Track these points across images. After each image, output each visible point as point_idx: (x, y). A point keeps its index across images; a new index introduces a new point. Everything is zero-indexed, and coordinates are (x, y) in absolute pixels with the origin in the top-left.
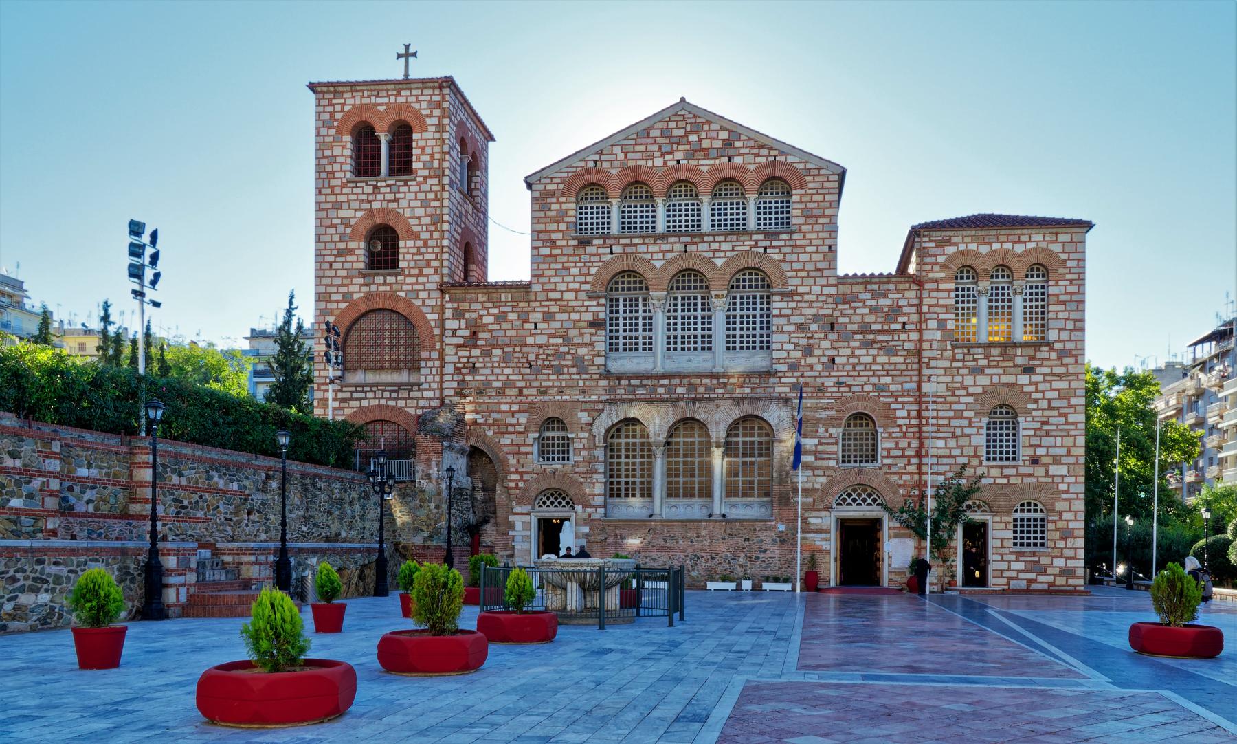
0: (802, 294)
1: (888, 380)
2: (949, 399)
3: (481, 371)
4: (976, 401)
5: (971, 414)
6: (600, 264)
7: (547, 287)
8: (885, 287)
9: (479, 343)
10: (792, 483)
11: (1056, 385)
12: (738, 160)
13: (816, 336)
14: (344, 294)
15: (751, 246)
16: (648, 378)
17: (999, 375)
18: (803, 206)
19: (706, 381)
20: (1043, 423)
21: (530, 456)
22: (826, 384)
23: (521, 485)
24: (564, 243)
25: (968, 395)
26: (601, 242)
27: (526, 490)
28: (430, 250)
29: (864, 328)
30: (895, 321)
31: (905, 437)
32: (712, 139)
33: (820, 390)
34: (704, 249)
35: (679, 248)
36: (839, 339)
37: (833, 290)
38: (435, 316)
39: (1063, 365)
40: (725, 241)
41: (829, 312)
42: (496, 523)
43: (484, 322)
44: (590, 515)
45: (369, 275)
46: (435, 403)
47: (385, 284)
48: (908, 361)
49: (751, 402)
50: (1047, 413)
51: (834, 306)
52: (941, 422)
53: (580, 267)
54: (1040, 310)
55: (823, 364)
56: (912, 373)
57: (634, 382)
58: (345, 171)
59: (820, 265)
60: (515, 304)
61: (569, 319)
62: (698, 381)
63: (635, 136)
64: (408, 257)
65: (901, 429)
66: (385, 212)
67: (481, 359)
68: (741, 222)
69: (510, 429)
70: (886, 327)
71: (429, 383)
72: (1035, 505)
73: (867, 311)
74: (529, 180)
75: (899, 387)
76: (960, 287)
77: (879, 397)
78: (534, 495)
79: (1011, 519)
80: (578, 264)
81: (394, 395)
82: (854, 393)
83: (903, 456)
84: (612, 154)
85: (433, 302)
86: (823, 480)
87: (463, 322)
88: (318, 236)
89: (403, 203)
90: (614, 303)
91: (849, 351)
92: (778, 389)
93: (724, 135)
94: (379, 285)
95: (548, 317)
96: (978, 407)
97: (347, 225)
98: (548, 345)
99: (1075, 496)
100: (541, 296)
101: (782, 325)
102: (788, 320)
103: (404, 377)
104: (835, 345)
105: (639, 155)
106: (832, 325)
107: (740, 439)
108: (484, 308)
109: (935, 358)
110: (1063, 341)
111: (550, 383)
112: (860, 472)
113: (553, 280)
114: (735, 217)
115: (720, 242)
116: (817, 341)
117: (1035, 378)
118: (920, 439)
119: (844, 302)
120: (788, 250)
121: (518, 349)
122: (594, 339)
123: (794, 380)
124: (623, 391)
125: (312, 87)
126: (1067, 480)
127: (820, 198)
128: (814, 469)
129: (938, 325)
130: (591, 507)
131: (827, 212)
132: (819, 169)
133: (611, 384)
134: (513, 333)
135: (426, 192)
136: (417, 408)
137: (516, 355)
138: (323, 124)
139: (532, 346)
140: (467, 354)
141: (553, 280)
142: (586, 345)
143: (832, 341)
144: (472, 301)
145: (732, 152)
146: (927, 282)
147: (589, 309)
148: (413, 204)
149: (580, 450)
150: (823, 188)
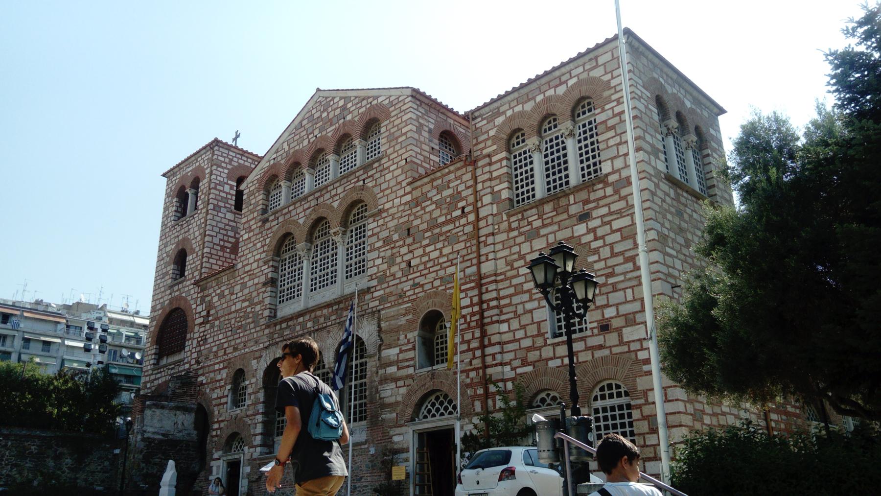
2: (509, 274)
3: (210, 340)
7: (245, 263)
8: (446, 179)
10: (380, 398)
12: (349, 117)
13: (397, 244)
15: (355, 183)
17: (554, 232)
18: (387, 133)
19: (325, 311)
20: (608, 276)
21: (225, 406)
22: (405, 290)
29: (433, 225)
30: (456, 209)
31: (469, 328)
33: (401, 296)
35: (313, 203)
36: (414, 242)
37: (408, 198)
39: (621, 199)
41: (406, 219)
44: (252, 455)
48: (468, 244)
50: (611, 262)
52: (503, 302)
55: (402, 270)
59: (399, 179)
62: (319, 313)
64: (189, 267)
65: (465, 320)
69: (218, 384)
70: (449, 217)
72: (618, 387)
73: (434, 206)
77: (445, 290)
78: (223, 441)
83: (469, 350)
86: (403, 390)
89: (191, 231)
91: (420, 252)
92: (371, 305)
93: (341, 103)
100: (241, 272)
104: (411, 248)
106: (409, 230)
109: (493, 234)
110: (619, 171)
112: (433, 375)
117: (593, 224)
118: (482, 325)
119: (417, 206)
121: (227, 318)
122: (265, 295)
123: (381, 292)
125: (164, 175)
127: (399, 121)
128: (396, 380)
129: (493, 199)
131: (404, 130)
132: (398, 98)
133: (271, 331)
138: (168, 195)
139: (234, 312)
145: (345, 113)
146: (480, 160)
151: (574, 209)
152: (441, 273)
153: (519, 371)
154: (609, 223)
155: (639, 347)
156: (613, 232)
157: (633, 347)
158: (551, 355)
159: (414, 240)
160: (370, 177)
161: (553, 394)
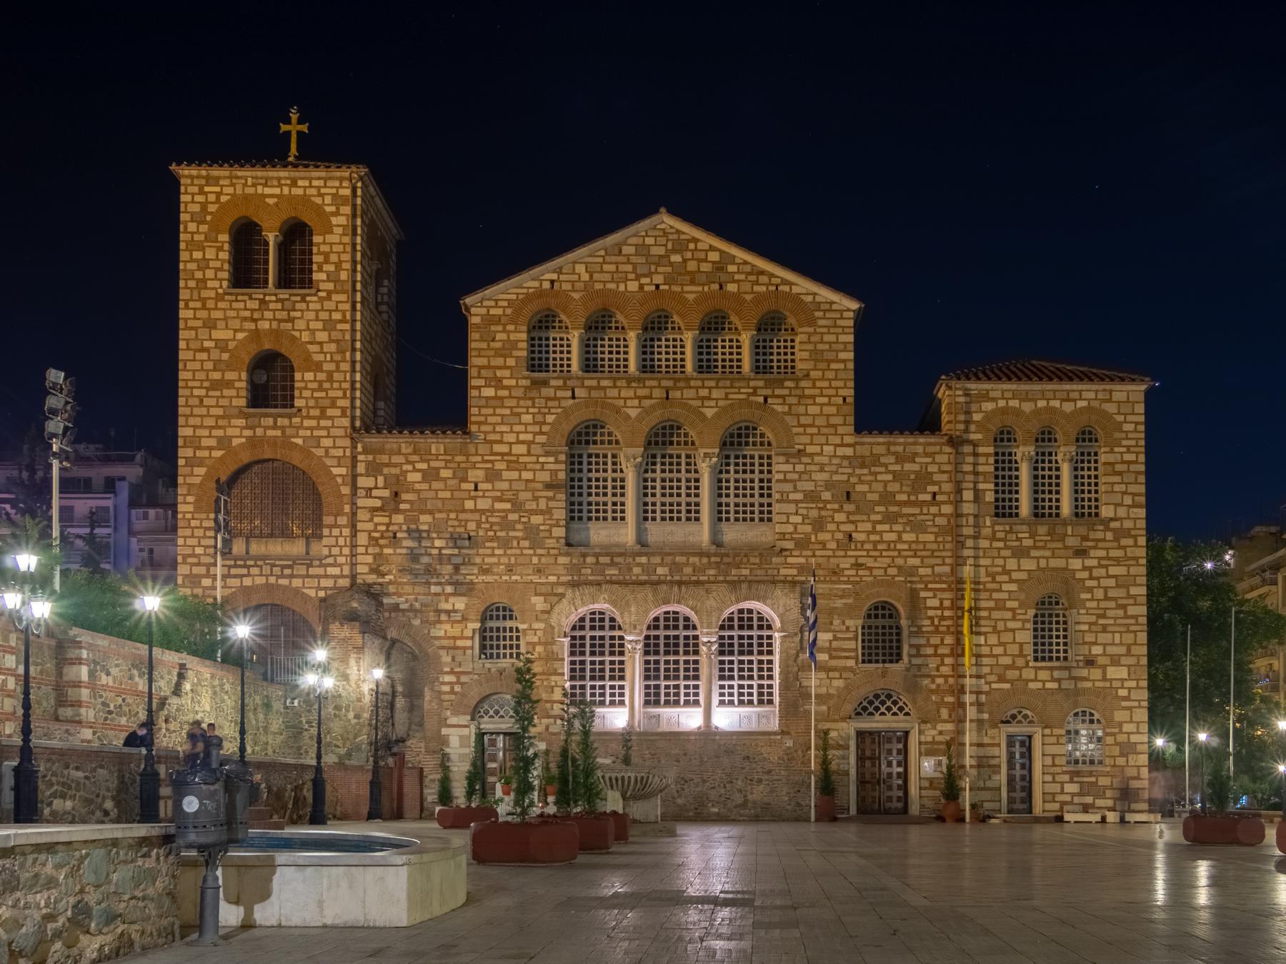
0: (812, 455)
1: (916, 561)
4: (1020, 589)
5: (1015, 604)
6: (559, 410)
7: (492, 437)
9: (402, 506)
11: (1113, 571)
12: (731, 288)
13: (829, 506)
14: (220, 439)
15: (749, 394)
16: (621, 555)
17: (1047, 558)
18: (811, 347)
20: (1099, 616)
22: (842, 566)
23: (457, 688)
24: (513, 382)
25: (1011, 581)
26: (560, 383)
27: (463, 695)
28: (336, 385)
29: (888, 498)
31: (937, 631)
32: (700, 261)
33: (835, 573)
34: (691, 396)
35: (658, 393)
36: (858, 511)
37: (849, 451)
39: (1120, 547)
40: (717, 387)
41: (845, 478)
42: (424, 737)
43: (409, 479)
45: (254, 415)
46: (344, 583)
47: (275, 427)
48: (940, 539)
49: (750, 588)
51: (850, 471)
53: (534, 414)
54: (1093, 481)
55: (838, 541)
56: (944, 554)
57: (603, 560)
58: (221, 280)
59: (834, 420)
60: (448, 458)
61: (520, 479)
63: (602, 253)
64: (307, 393)
65: (933, 622)
66: (276, 334)
68: (735, 364)
70: (913, 498)
71: (335, 556)
72: (1092, 715)
73: (890, 477)
75: (929, 571)
76: (1000, 451)
77: (906, 582)
79: (1063, 732)
80: (531, 410)
81: (287, 572)
82: (875, 577)
83: (936, 655)
84: (574, 273)
85: (340, 453)
86: (837, 683)
87: (381, 480)
89: (300, 324)
90: (576, 459)
91: (868, 526)
92: (783, 572)
93: (714, 256)
94: (266, 428)
95: (493, 476)
96: (1023, 596)
97: (224, 350)
98: (492, 511)
99: (1136, 704)
101: (788, 493)
102: (795, 487)
103: (297, 548)
105: (608, 277)
106: (848, 493)
107: (735, 633)
108: (408, 462)
110: (1120, 519)
111: (494, 560)
113: (498, 429)
114: (727, 357)
115: (710, 388)
116: (830, 513)
117: (1089, 563)
119: (863, 466)
120: (793, 400)
121: (453, 516)
122: (551, 504)
123: (802, 560)
124: (589, 571)
126: (1127, 684)
128: (828, 670)
130: (549, 717)
134: (448, 495)
135: (330, 311)
136: (319, 588)
137: (450, 523)
139: (471, 511)
140: (386, 520)
141: (498, 429)
142: (542, 512)
143: (849, 513)
144: (392, 453)
147: (546, 466)
148: (313, 325)
149: (534, 645)
150: (835, 326)
151: (1071, 541)
152: (900, 561)
153: (994, 686)
154: (1106, 567)
155: (1119, 684)
156: (1109, 576)
157: (1115, 684)
158: (1032, 677)
159: (858, 508)
160: (777, 397)
161: (1025, 712)
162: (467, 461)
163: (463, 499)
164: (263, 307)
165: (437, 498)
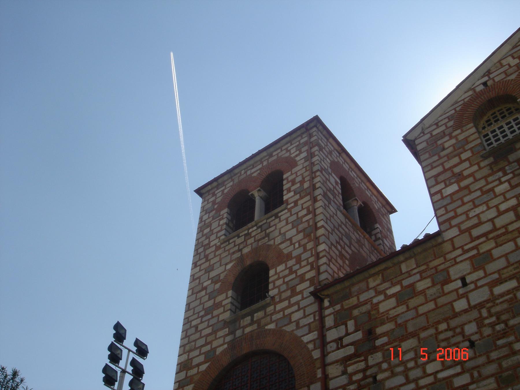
14: (206, 353)
28: (304, 263)
38: (314, 335)
47: (252, 322)
53: (508, 181)
60: (423, 268)
64: (279, 282)
66: (255, 251)
67: (385, 366)
74: (409, 138)
85: (311, 319)
87: (351, 324)
88: (188, 305)
98: (493, 299)
121: (443, 326)
137: (442, 337)
139: (465, 311)
162: (446, 261)
163: (451, 303)
164: (247, 238)
165: (418, 316)
